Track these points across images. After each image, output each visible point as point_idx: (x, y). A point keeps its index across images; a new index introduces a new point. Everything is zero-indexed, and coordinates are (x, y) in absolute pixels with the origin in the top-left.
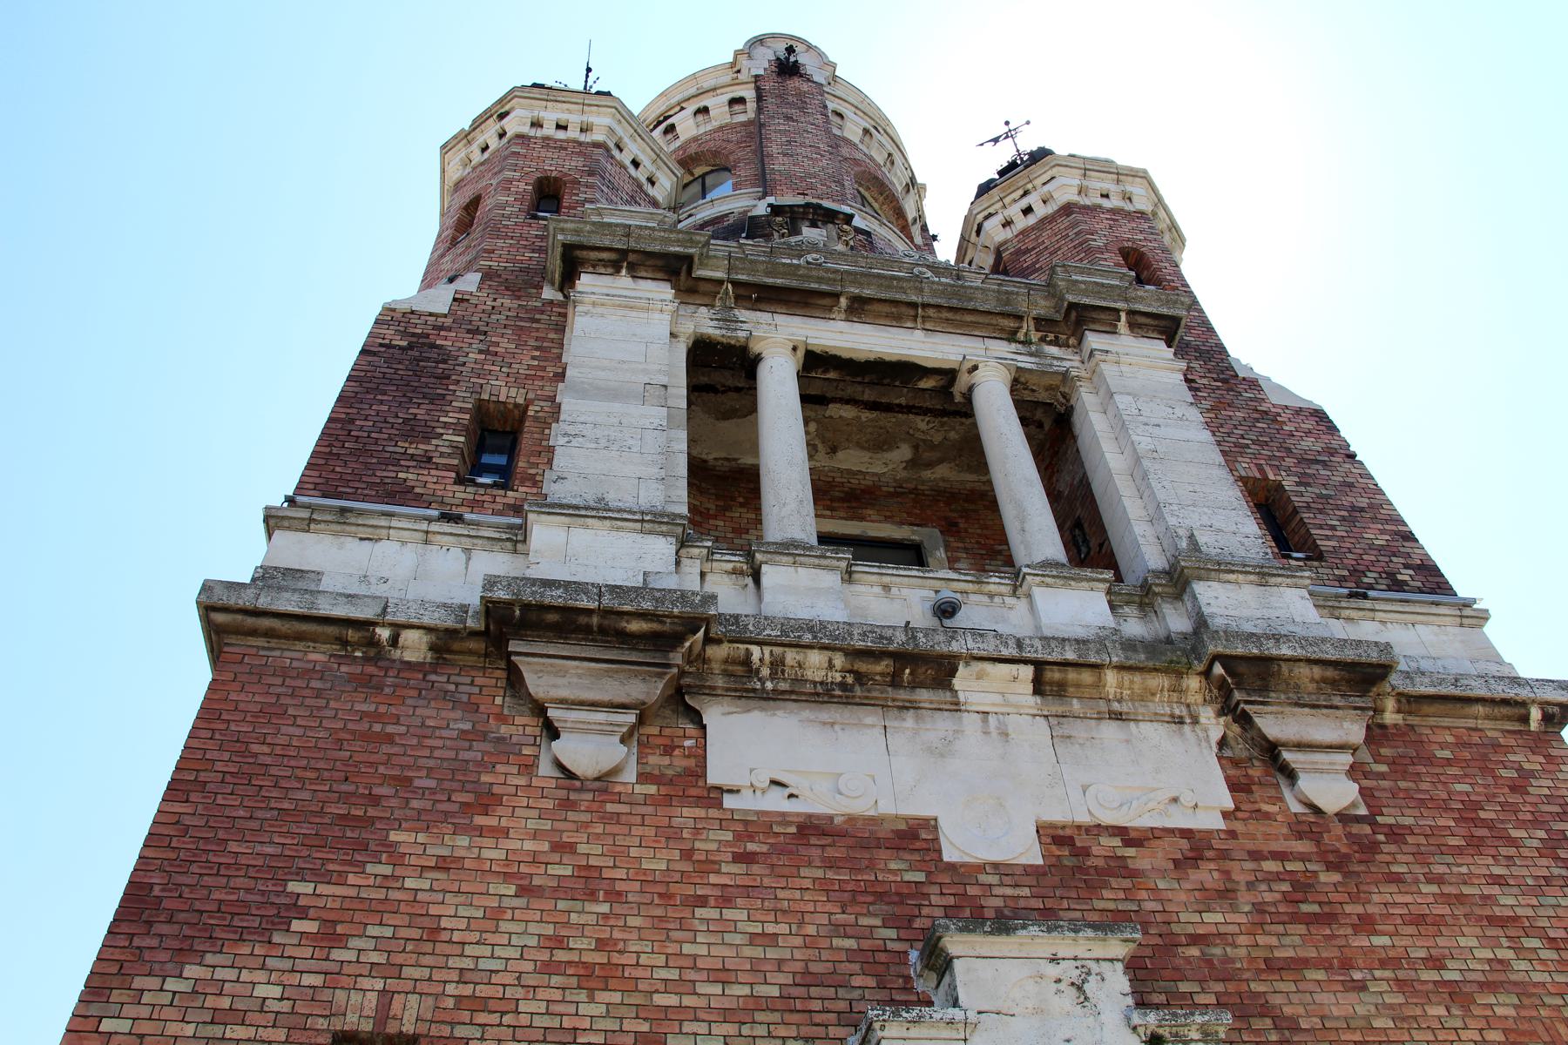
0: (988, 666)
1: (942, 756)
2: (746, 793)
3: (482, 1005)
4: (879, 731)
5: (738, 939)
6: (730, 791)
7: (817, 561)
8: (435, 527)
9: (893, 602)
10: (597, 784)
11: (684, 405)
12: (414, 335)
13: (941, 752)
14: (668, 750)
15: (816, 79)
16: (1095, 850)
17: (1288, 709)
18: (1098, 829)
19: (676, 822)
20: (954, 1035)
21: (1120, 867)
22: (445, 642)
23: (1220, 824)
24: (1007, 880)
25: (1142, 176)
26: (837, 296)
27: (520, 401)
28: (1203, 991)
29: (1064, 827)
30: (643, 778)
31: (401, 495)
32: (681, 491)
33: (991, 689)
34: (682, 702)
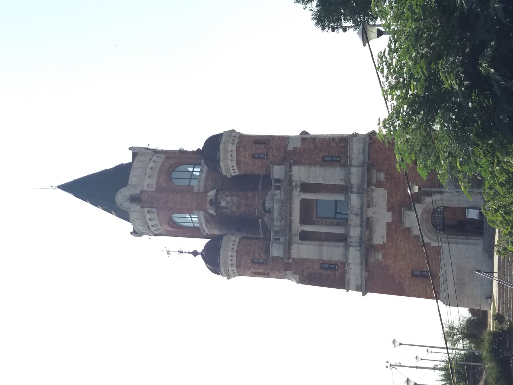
18: (387, 205)
23: (386, 191)
33: (369, 213)
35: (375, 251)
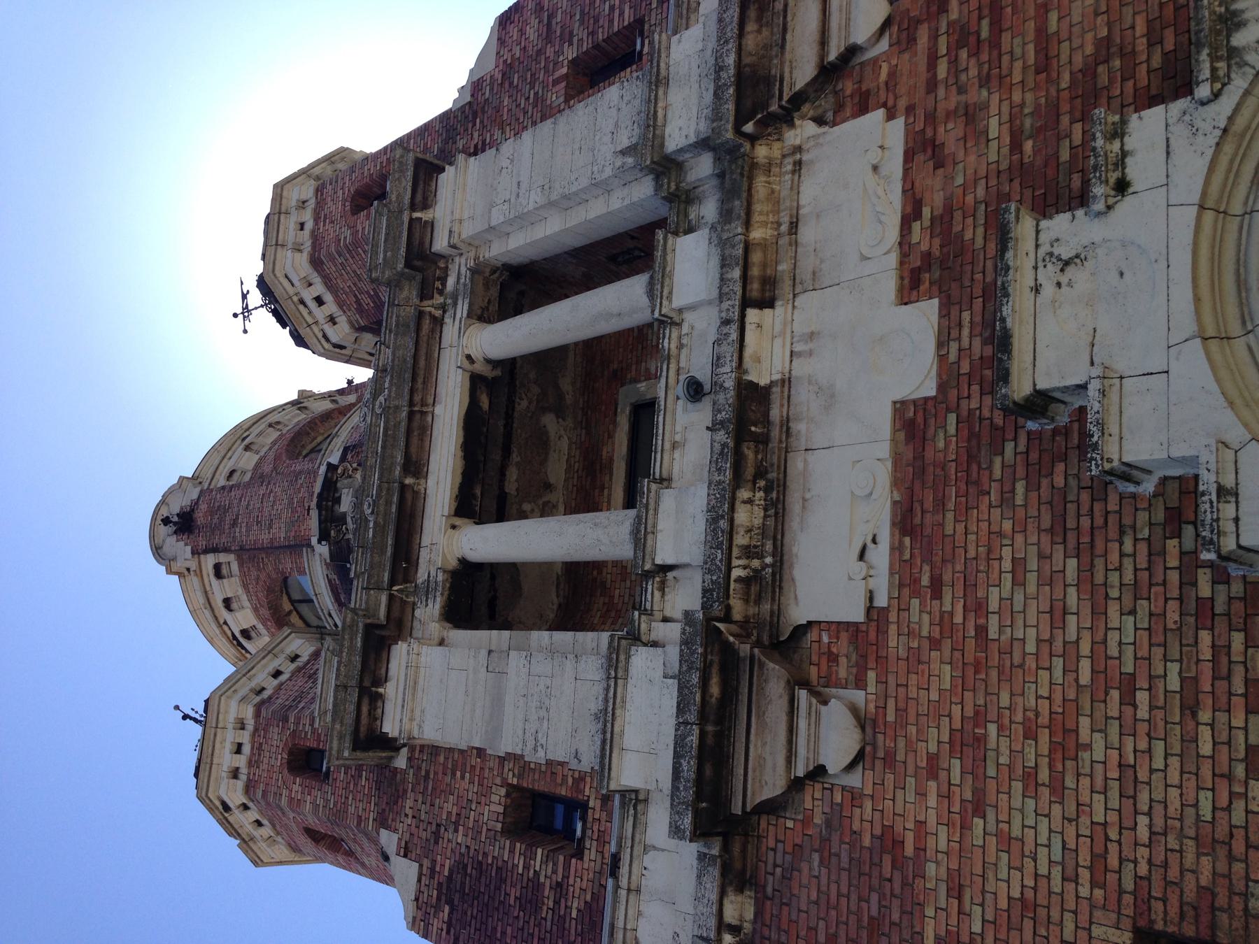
0: (748, 353)
1: (833, 396)
2: (872, 583)
3: (1098, 859)
4: (811, 457)
5: (1019, 598)
6: (871, 596)
7: (651, 512)
8: (624, 882)
9: (689, 441)
10: (869, 730)
11: (506, 633)
12: (439, 899)
13: (829, 397)
14: (833, 658)
15: (195, 496)
16: (924, 247)
17: (788, 56)
18: (904, 243)
19: (903, 653)
20: (1116, 388)
21: (942, 224)
22: (735, 875)
24: (954, 334)
25: (280, 189)
26: (403, 487)
27: (503, 791)
28: (1069, 136)
29: (902, 278)
30: (860, 684)
31: (593, 913)
32: (587, 638)
33: (769, 348)
34: (787, 644)
35: (798, 681)
